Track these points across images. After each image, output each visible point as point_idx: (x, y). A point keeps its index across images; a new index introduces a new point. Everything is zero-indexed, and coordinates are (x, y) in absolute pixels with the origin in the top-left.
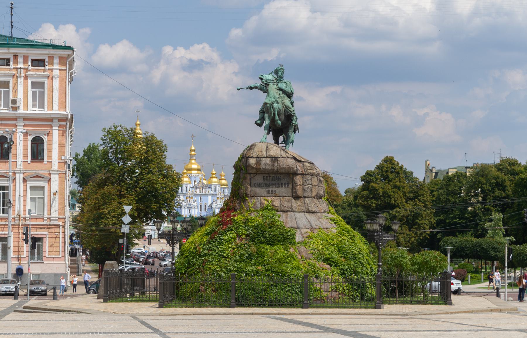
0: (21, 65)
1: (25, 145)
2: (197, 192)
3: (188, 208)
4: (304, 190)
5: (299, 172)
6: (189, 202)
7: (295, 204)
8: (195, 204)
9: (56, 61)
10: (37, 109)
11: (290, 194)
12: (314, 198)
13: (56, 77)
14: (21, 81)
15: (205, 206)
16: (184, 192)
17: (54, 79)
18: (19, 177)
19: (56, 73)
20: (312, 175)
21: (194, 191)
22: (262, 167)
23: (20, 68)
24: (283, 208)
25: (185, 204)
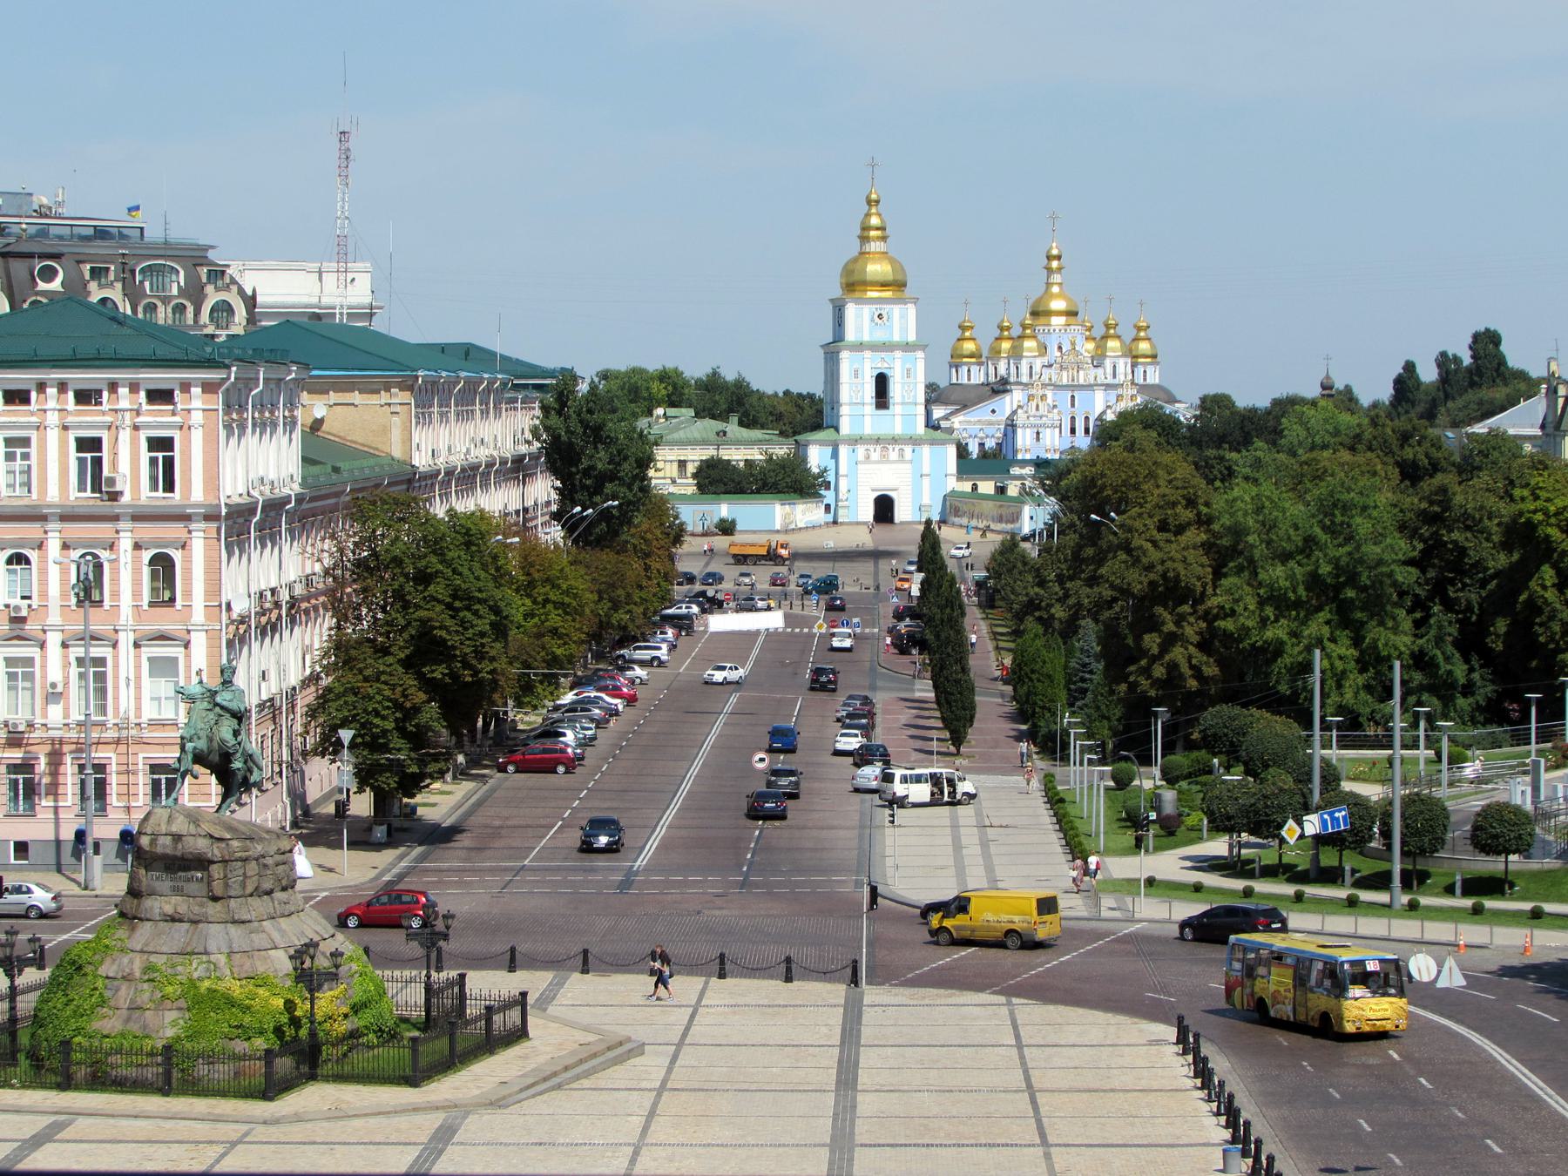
0: (124, 403)
1: (137, 571)
3: (1032, 426)
4: (227, 885)
7: (214, 909)
8: (1055, 414)
9: (196, 391)
12: (251, 895)
14: (125, 436)
15: (1087, 419)
16: (1025, 379)
18: (126, 639)
19: (197, 417)
20: (245, 860)
22: (159, 850)
23: (124, 410)
24: (192, 916)
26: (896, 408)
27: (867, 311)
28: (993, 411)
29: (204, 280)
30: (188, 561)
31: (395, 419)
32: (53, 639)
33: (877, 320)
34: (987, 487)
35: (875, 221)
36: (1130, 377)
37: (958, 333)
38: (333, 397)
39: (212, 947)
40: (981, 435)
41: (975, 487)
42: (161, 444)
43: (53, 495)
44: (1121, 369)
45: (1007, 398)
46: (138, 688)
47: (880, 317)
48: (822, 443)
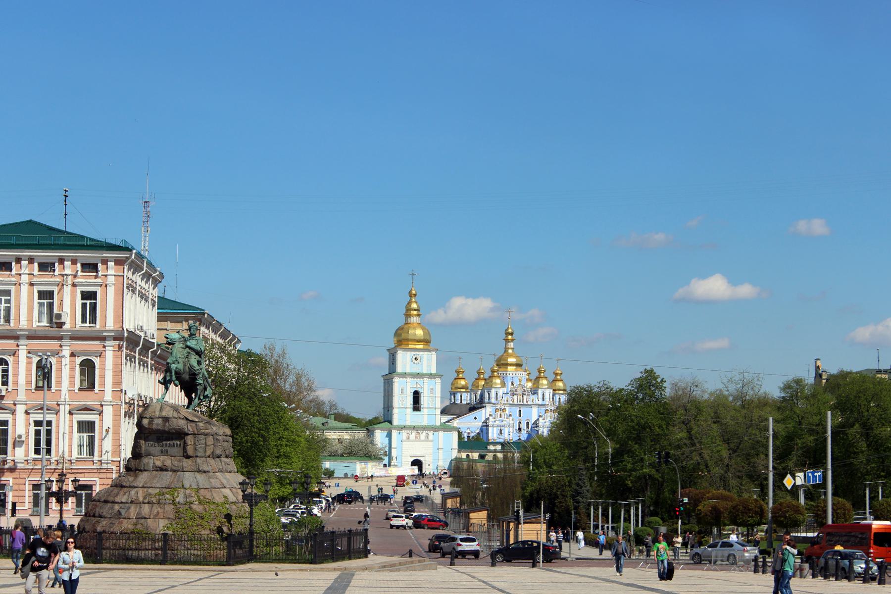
1: (72, 369)
2: (513, 401)
4: (195, 449)
5: (189, 433)
6: (501, 417)
7: (187, 463)
10: (88, 324)
11: (181, 454)
12: (209, 457)
13: (110, 285)
14: (67, 290)
17: (108, 287)
19: (111, 280)
21: (510, 399)
25: (494, 420)
28: (475, 418)
30: (103, 363)
32: (21, 409)
37: (455, 375)
39: (187, 485)
40: (468, 431)
42: (89, 296)
43: (24, 324)
44: (547, 396)
46: (71, 439)
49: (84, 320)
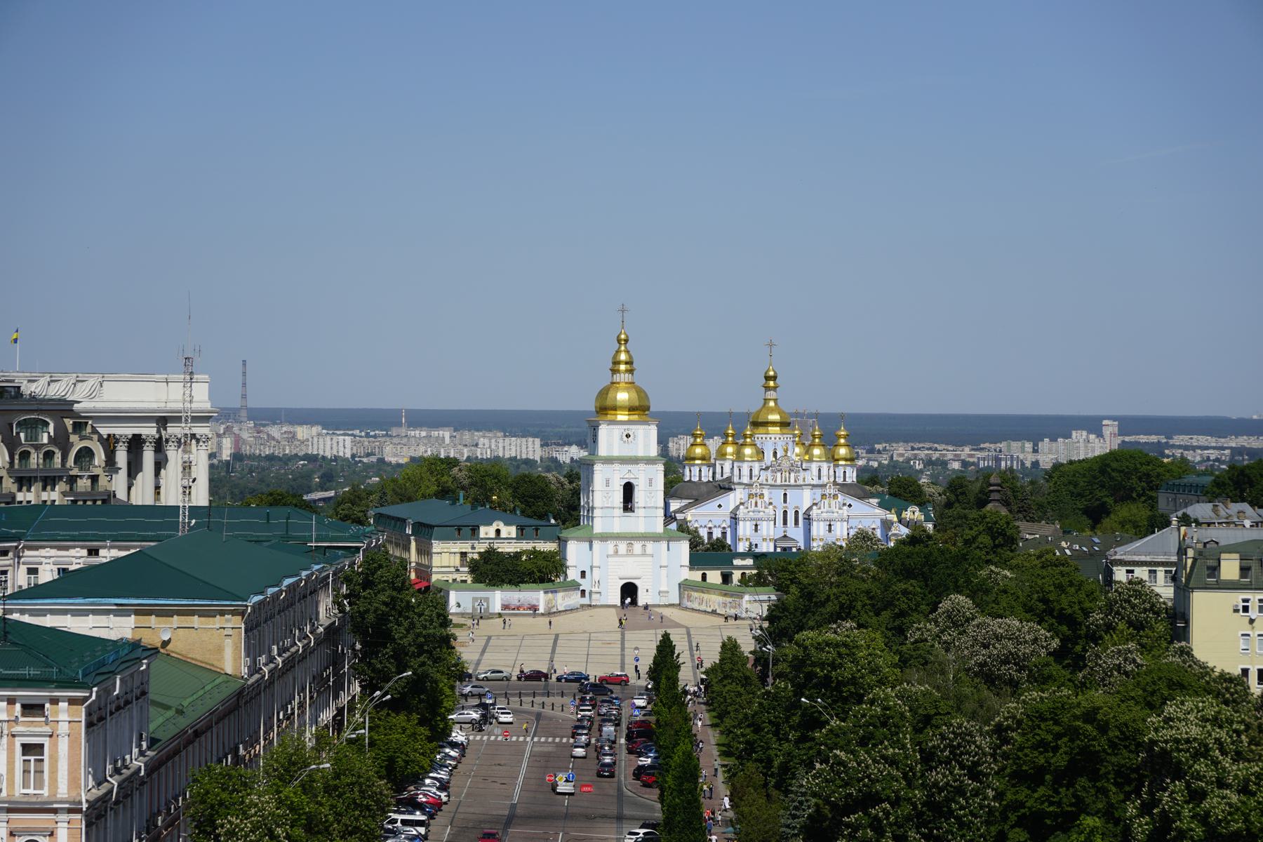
2: (776, 481)
3: (752, 520)
6: (756, 505)
15: (797, 513)
16: (745, 480)
19: (63, 728)
26: (639, 512)
27: (617, 431)
28: (720, 506)
29: (70, 430)
31: (229, 641)
33: (625, 438)
34: (714, 577)
35: (623, 357)
36: (832, 479)
38: (176, 620)
40: (710, 525)
41: (704, 577)
45: (731, 495)
47: (628, 436)
48: (579, 539)
49: (25, 785)
